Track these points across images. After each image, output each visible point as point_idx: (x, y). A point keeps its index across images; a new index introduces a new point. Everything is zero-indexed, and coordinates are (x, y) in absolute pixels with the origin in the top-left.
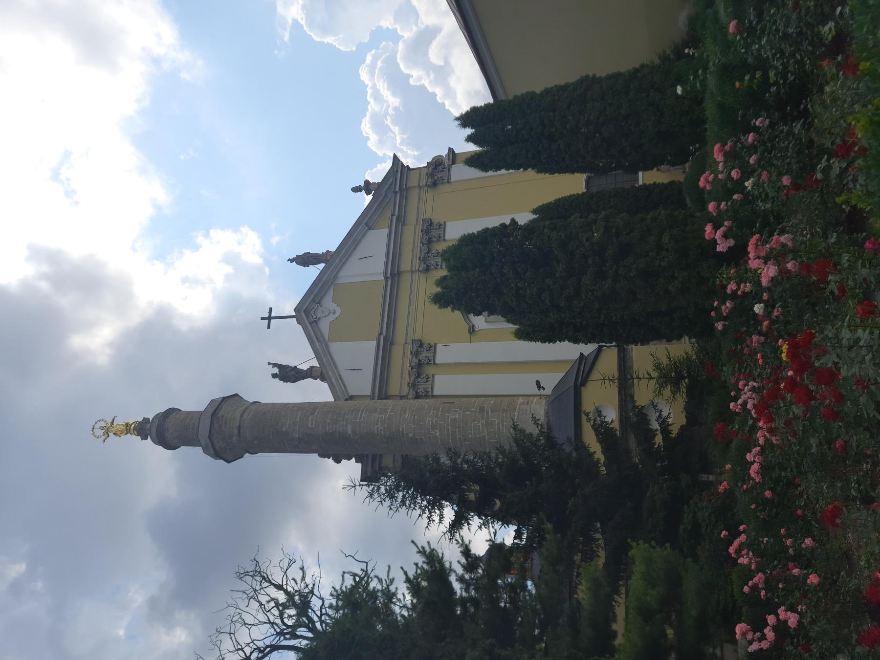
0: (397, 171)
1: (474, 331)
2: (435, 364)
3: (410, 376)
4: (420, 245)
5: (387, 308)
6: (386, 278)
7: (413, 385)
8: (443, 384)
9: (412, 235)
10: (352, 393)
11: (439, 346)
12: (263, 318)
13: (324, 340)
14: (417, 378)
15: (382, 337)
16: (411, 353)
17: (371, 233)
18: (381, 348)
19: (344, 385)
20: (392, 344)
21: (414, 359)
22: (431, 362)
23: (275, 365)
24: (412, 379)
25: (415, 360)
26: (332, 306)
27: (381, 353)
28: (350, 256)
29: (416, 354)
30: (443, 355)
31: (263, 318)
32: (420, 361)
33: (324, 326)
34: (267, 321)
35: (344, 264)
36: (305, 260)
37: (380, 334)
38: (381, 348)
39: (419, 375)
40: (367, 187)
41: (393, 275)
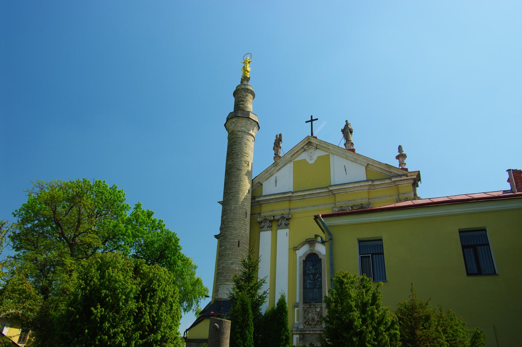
0: (407, 176)
1: (296, 250)
2: (277, 229)
3: (270, 216)
4: (351, 204)
5: (309, 193)
6: (327, 188)
7: (265, 219)
8: (265, 236)
9: (360, 198)
10: (265, 184)
11: (287, 230)
12: (312, 116)
13: (294, 159)
14: (270, 221)
15: (290, 194)
16: (282, 214)
17: (364, 168)
18: (284, 196)
19: (268, 179)
20: (290, 200)
21: (279, 217)
22: (280, 227)
23: (280, 135)
24: (269, 218)
25: (277, 218)
26: (315, 157)
27: (281, 196)
28: (347, 159)
29: (283, 218)
30: (283, 234)
31: (312, 116)
32: (279, 220)
33: (304, 156)
34: (310, 119)
35: (341, 157)
36: (347, 131)
37: (293, 193)
38: (284, 196)
39: (271, 221)
40: (401, 156)
41: (330, 191)
